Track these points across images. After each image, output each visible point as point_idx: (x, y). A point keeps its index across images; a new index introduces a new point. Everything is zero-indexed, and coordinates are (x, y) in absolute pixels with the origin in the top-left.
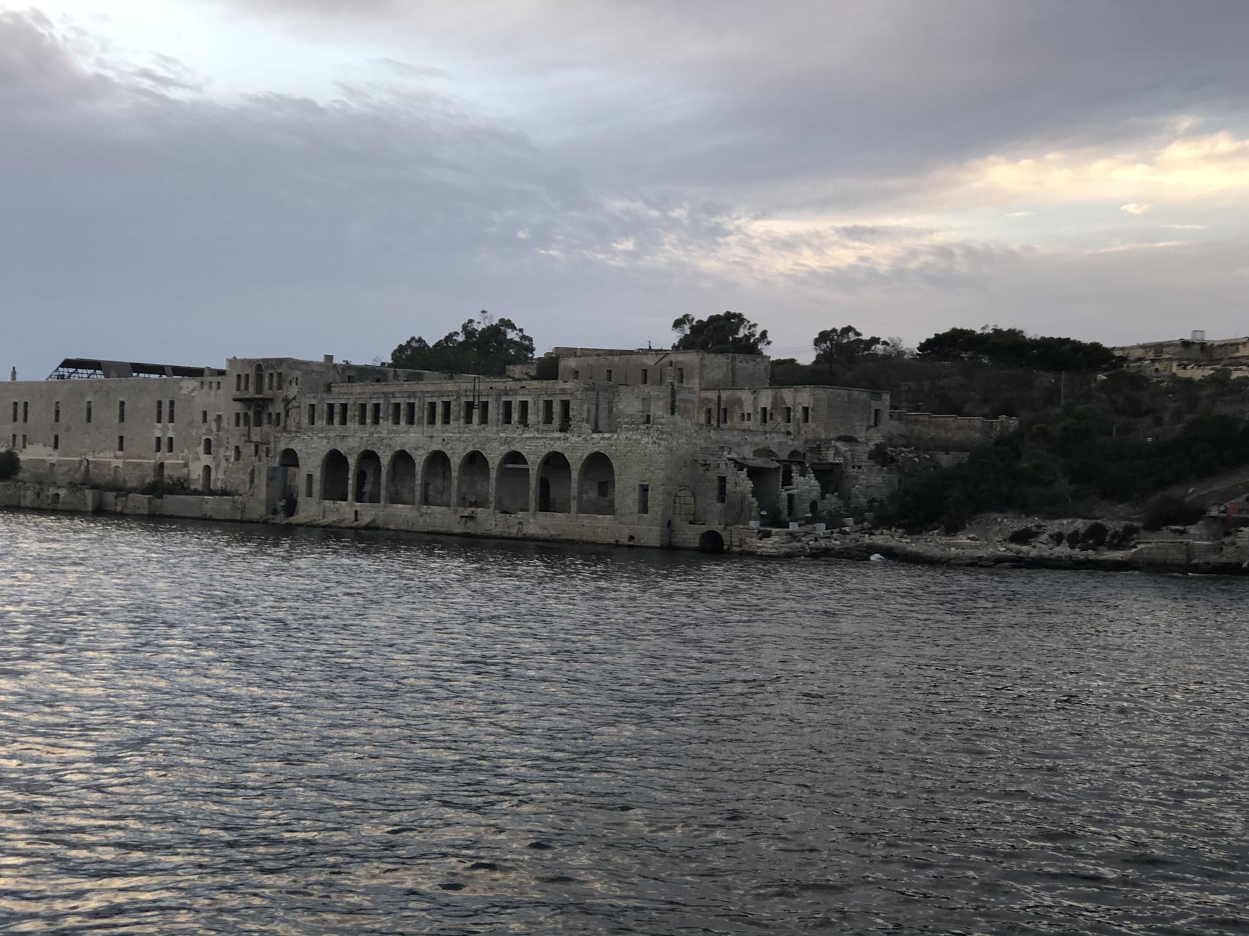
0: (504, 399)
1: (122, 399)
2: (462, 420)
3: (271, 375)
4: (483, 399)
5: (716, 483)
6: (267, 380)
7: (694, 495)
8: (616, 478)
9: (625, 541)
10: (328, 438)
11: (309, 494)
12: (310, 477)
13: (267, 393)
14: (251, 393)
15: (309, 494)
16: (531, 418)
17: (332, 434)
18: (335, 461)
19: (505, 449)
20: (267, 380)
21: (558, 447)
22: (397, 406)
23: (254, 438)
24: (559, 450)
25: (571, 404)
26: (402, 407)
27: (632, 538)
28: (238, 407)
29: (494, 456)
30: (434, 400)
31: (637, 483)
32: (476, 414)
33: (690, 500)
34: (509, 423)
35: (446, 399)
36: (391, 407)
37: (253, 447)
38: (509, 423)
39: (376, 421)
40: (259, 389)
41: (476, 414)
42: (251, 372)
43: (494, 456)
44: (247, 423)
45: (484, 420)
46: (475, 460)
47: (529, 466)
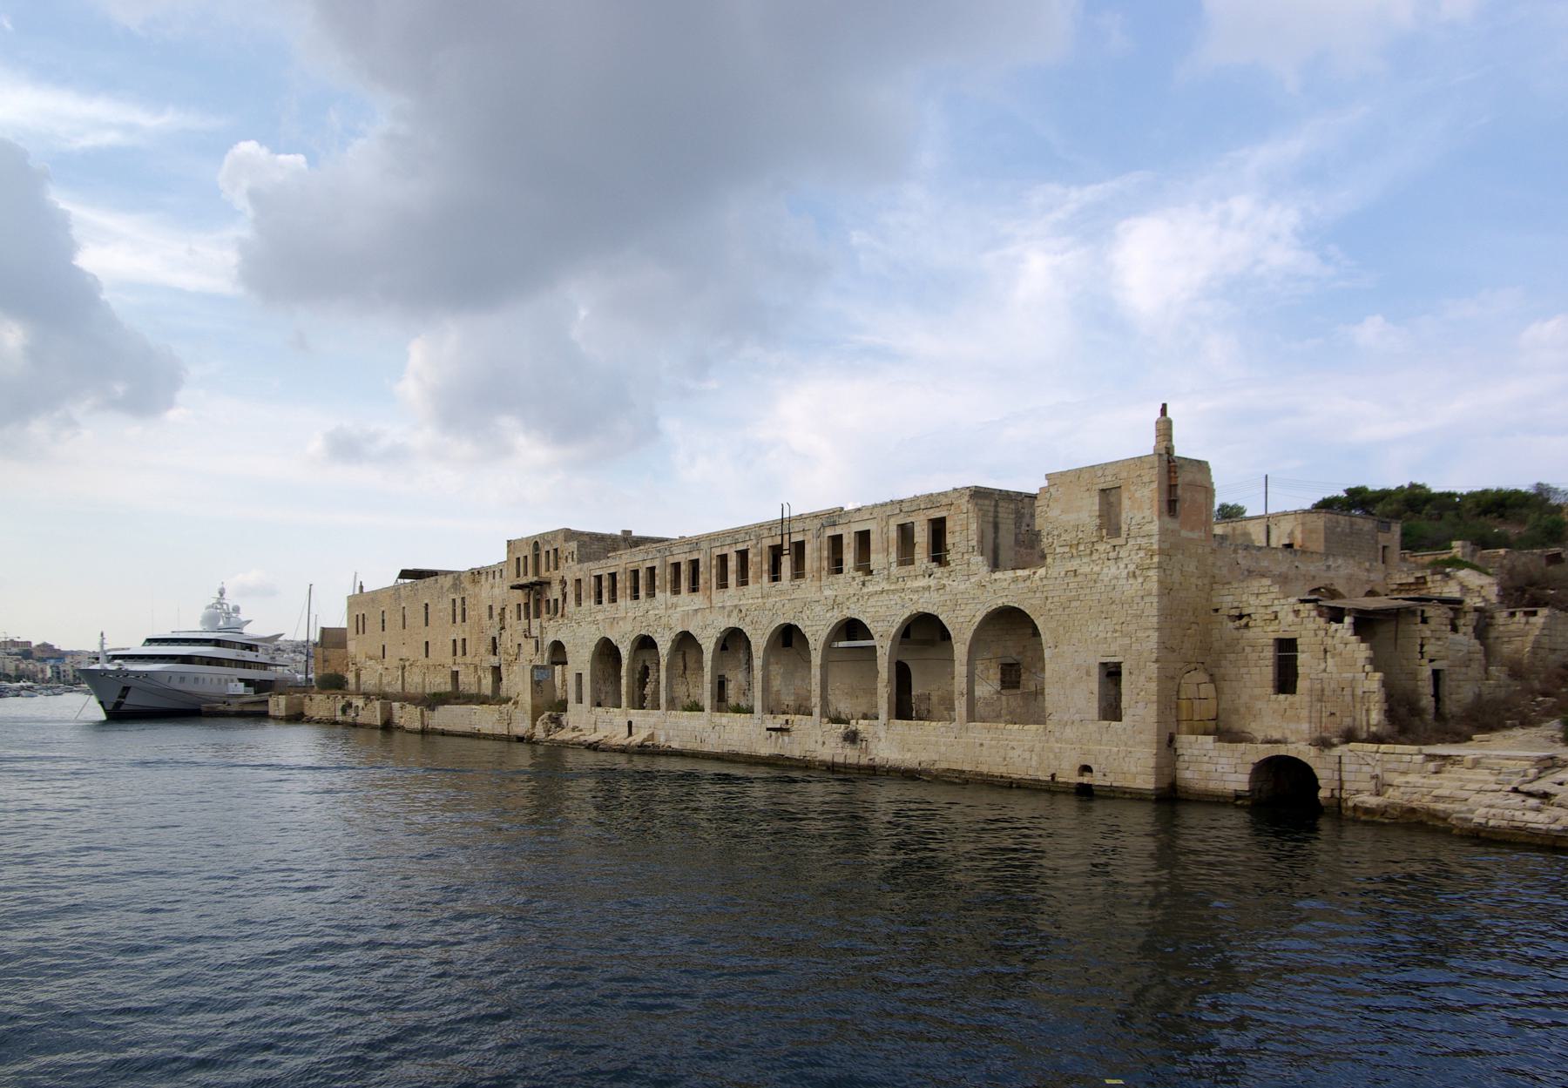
0: (830, 532)
2: (765, 577)
4: (796, 538)
5: (1269, 654)
6: (543, 559)
7: (1212, 679)
8: (1047, 653)
10: (595, 622)
11: (580, 700)
13: (544, 574)
14: (531, 578)
15: (580, 700)
16: (876, 560)
17: (600, 617)
18: (607, 652)
19: (836, 616)
20: (543, 559)
21: (927, 603)
22: (677, 566)
24: (930, 610)
25: (949, 524)
26: (683, 567)
28: (519, 596)
29: (816, 630)
30: (725, 551)
31: (1094, 661)
33: (1207, 690)
34: (840, 571)
35: (741, 547)
36: (668, 570)
37: (533, 642)
38: (840, 571)
41: (786, 563)
42: (528, 551)
43: (816, 630)
44: (527, 616)
45: (799, 571)
47: (876, 642)
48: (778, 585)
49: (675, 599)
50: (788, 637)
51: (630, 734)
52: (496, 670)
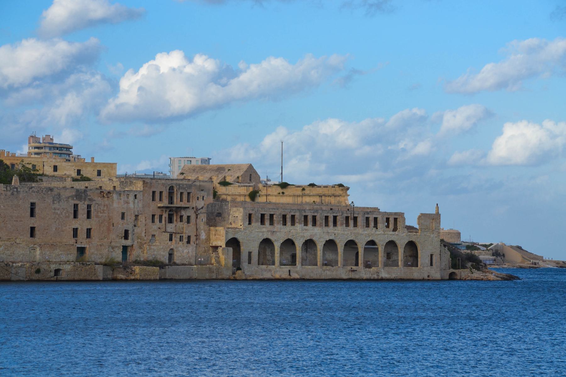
0: (366, 216)
1: (32, 201)
2: (344, 225)
3: (181, 193)
4: (356, 215)
9: (426, 277)
12: (250, 253)
13: (177, 203)
14: (165, 203)
23: (169, 230)
24: (395, 240)
27: (428, 276)
30: (328, 215)
32: (351, 222)
36: (303, 217)
37: (168, 235)
39: (293, 224)
40: (171, 201)
41: (351, 222)
45: (355, 225)
46: (331, 244)
48: (348, 228)
49: (305, 227)
50: (289, 243)
51: (290, 275)
52: (125, 248)
